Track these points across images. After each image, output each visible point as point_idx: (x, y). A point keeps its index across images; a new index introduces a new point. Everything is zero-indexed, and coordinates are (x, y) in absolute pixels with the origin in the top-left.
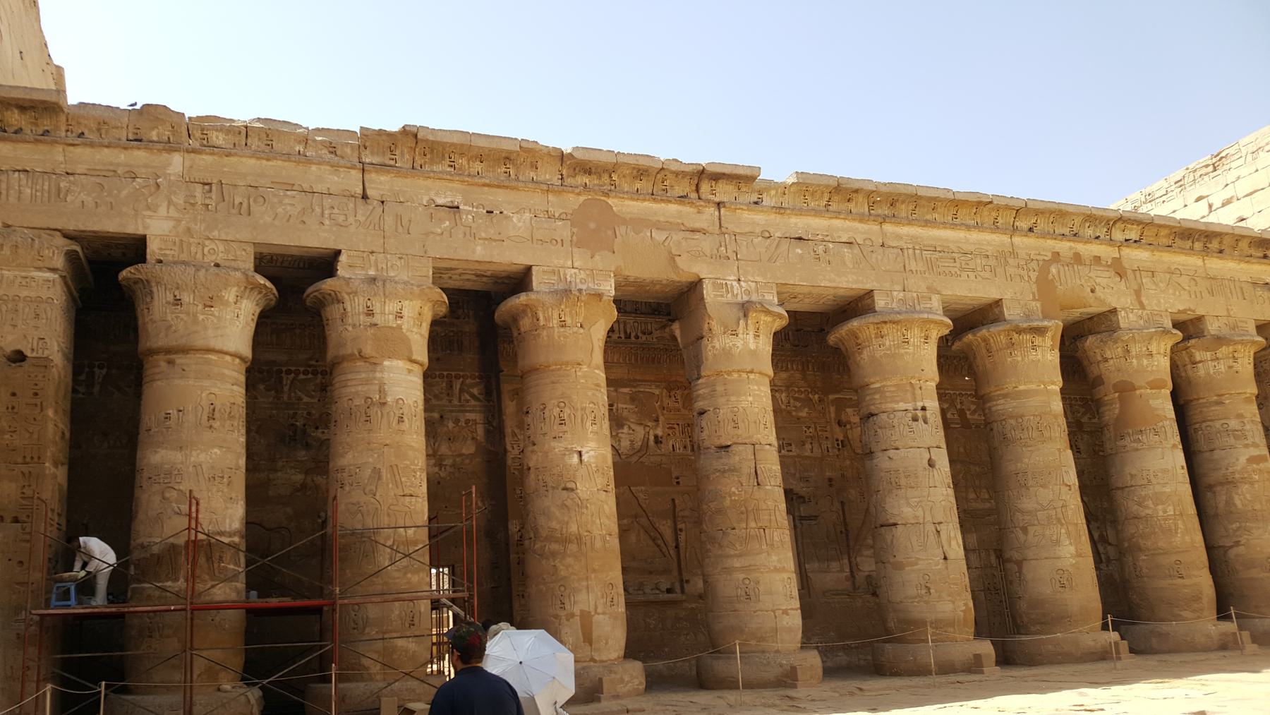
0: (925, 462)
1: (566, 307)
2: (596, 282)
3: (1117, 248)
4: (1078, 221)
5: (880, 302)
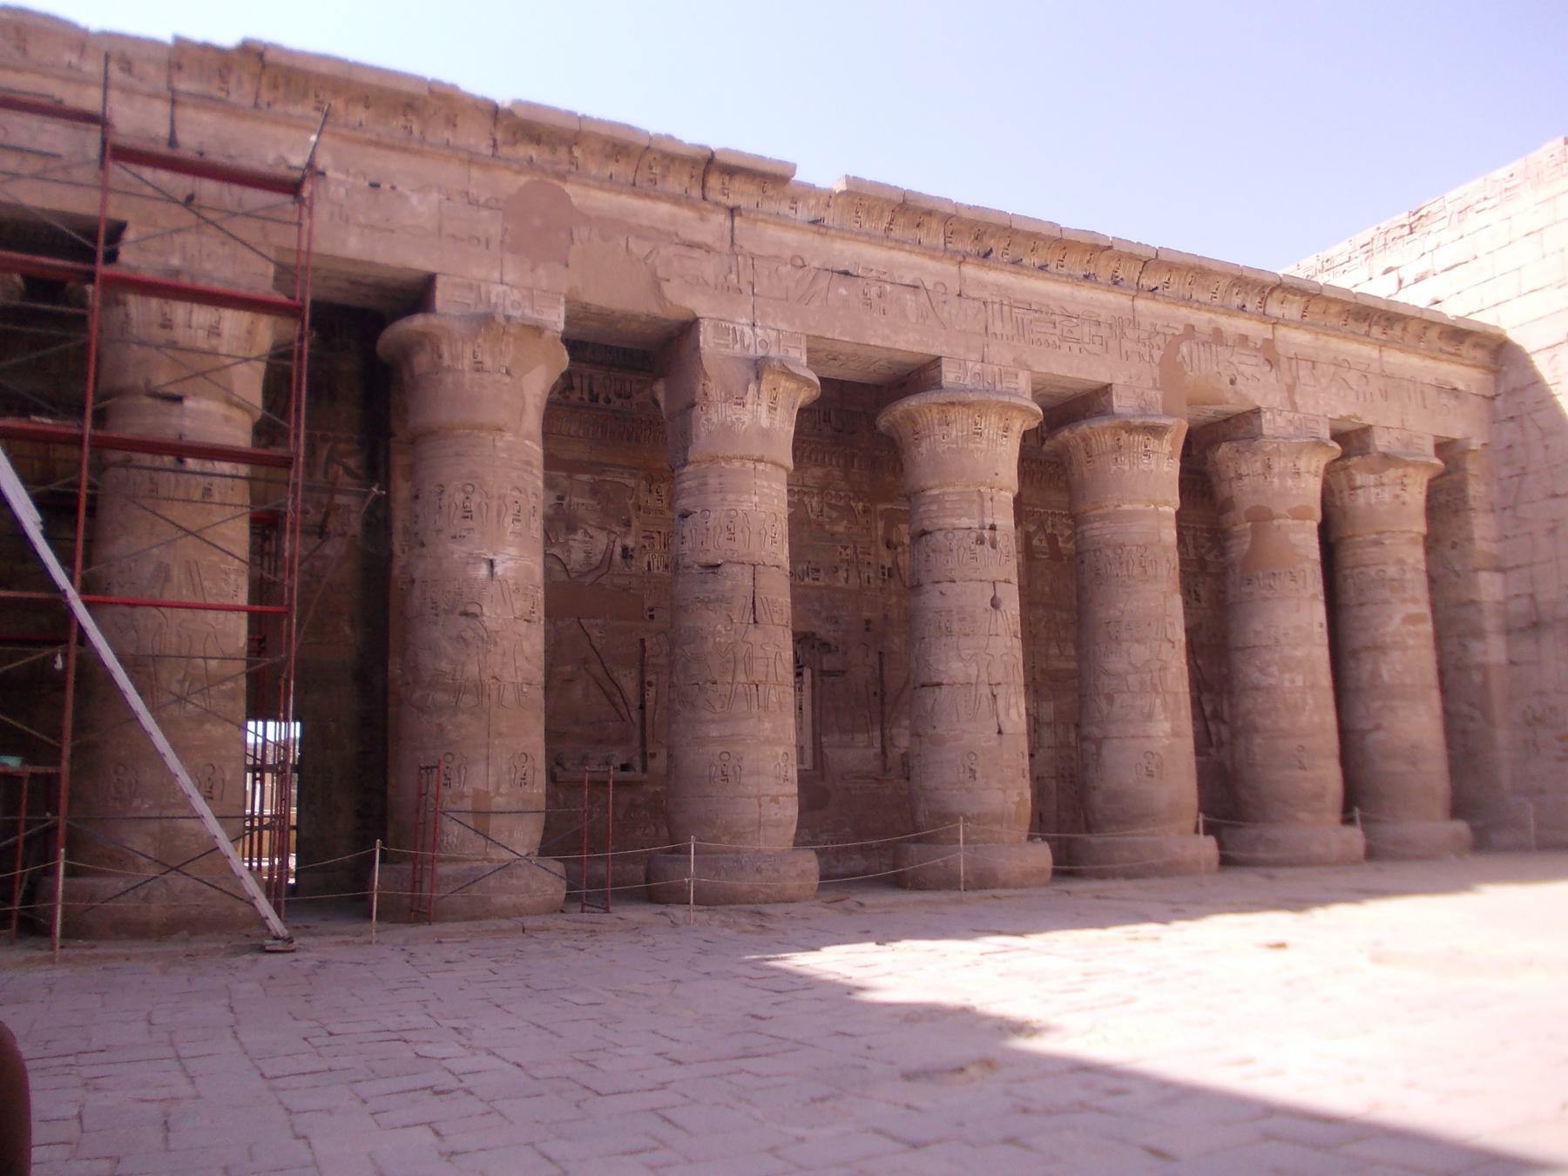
0: (988, 600)
1: (485, 340)
2: (537, 308)
3: (1270, 326)
4: (1224, 283)
5: (949, 375)
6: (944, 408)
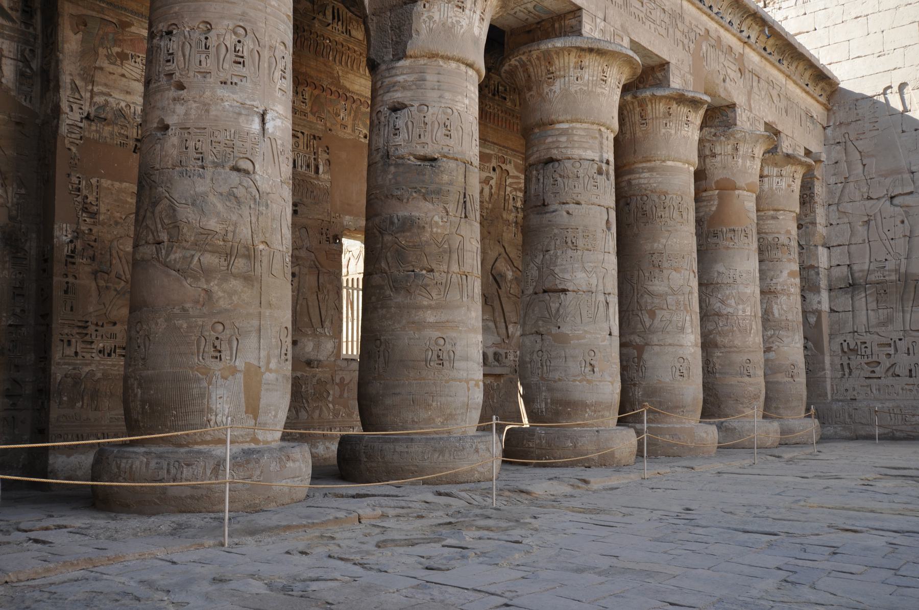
0: (604, 222)
6: (583, 53)
